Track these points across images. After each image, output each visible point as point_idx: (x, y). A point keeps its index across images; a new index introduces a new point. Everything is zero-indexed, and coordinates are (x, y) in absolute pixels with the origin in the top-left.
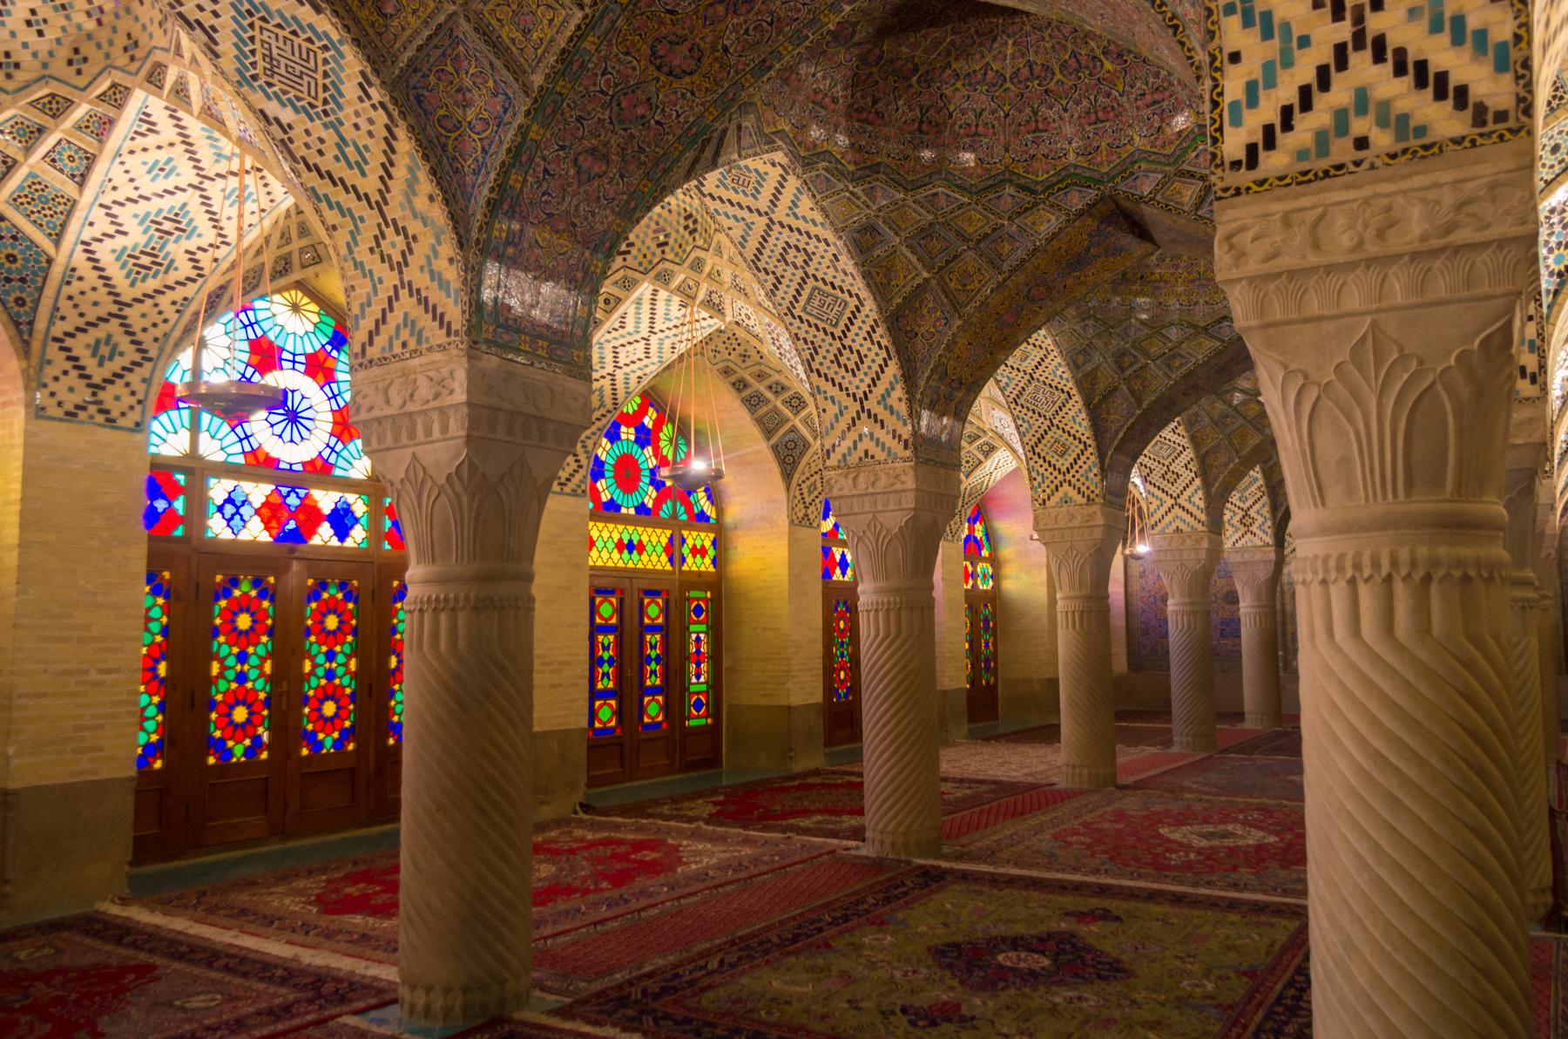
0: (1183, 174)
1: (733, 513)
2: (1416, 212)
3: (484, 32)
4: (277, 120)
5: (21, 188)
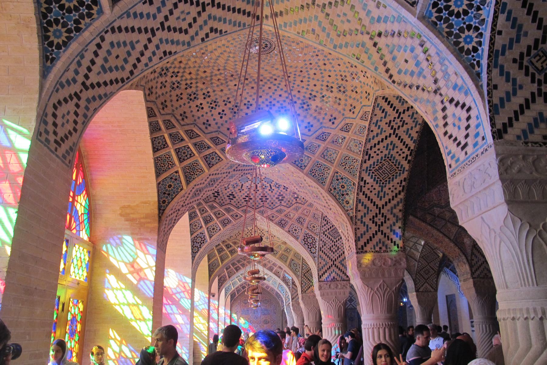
4: (365, 181)
5: (190, 164)
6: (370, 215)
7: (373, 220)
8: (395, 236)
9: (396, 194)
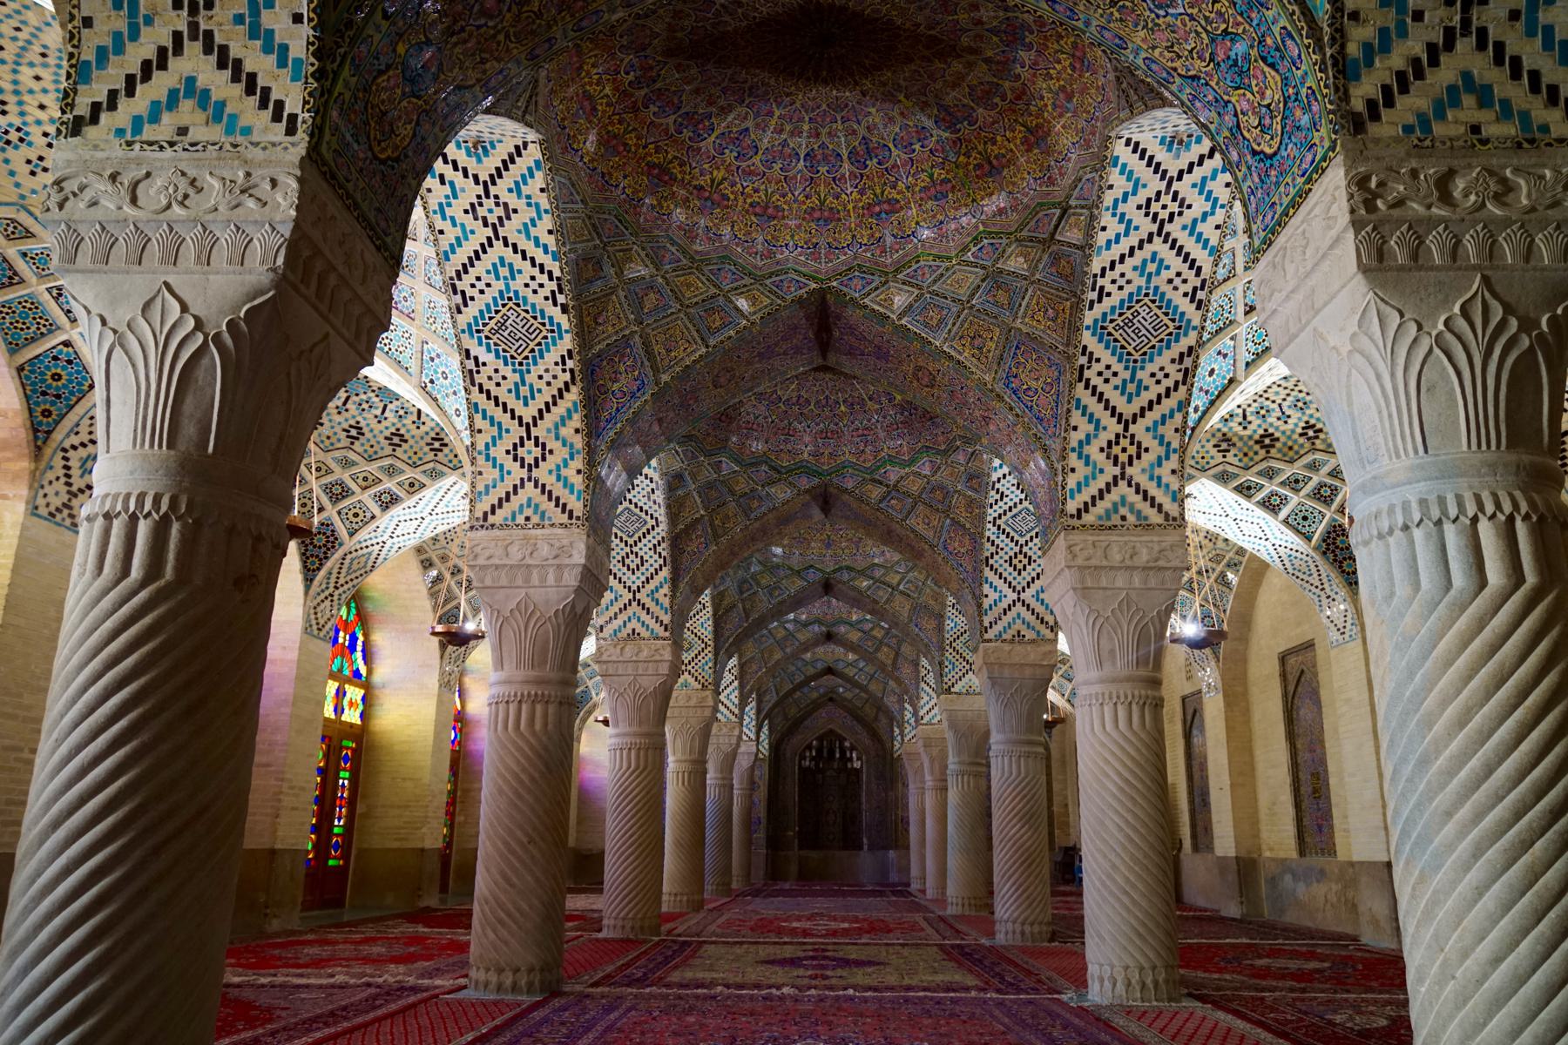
0: (874, 480)
1: (382, 673)
2: (1145, 551)
3: (647, 345)
4: (476, 359)
6: (507, 442)
7: (513, 452)
8: (567, 491)
9: (560, 390)
